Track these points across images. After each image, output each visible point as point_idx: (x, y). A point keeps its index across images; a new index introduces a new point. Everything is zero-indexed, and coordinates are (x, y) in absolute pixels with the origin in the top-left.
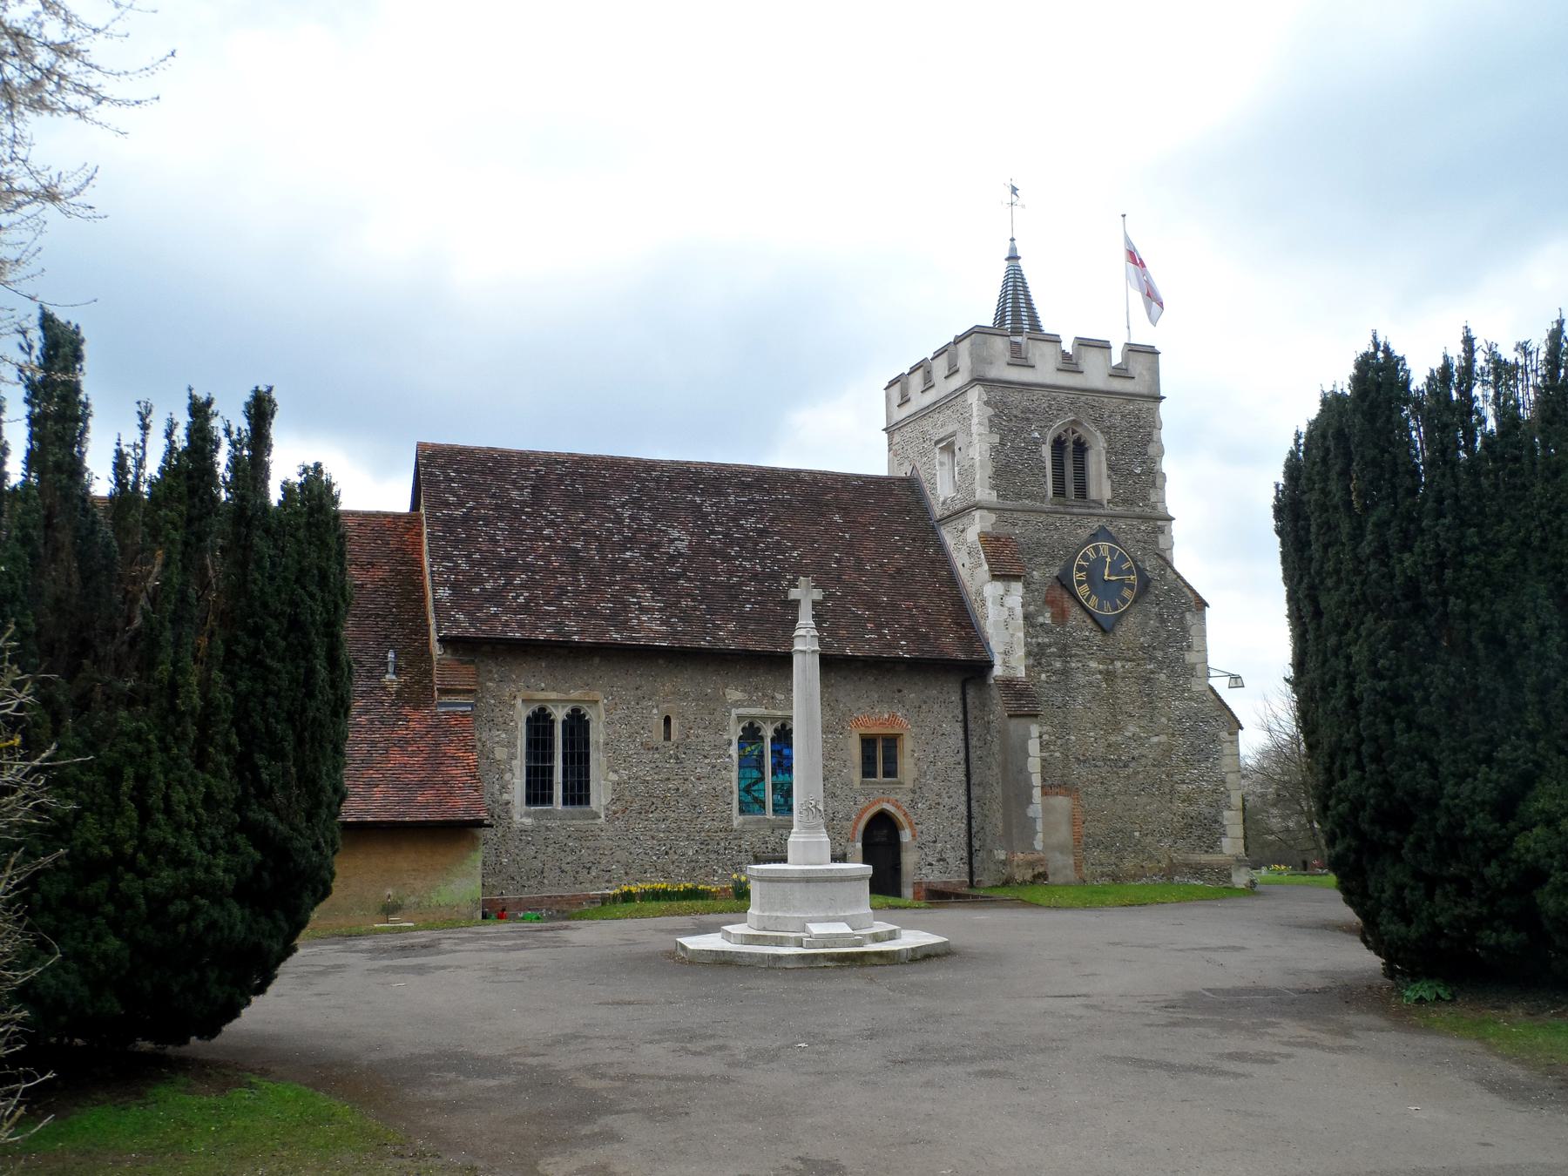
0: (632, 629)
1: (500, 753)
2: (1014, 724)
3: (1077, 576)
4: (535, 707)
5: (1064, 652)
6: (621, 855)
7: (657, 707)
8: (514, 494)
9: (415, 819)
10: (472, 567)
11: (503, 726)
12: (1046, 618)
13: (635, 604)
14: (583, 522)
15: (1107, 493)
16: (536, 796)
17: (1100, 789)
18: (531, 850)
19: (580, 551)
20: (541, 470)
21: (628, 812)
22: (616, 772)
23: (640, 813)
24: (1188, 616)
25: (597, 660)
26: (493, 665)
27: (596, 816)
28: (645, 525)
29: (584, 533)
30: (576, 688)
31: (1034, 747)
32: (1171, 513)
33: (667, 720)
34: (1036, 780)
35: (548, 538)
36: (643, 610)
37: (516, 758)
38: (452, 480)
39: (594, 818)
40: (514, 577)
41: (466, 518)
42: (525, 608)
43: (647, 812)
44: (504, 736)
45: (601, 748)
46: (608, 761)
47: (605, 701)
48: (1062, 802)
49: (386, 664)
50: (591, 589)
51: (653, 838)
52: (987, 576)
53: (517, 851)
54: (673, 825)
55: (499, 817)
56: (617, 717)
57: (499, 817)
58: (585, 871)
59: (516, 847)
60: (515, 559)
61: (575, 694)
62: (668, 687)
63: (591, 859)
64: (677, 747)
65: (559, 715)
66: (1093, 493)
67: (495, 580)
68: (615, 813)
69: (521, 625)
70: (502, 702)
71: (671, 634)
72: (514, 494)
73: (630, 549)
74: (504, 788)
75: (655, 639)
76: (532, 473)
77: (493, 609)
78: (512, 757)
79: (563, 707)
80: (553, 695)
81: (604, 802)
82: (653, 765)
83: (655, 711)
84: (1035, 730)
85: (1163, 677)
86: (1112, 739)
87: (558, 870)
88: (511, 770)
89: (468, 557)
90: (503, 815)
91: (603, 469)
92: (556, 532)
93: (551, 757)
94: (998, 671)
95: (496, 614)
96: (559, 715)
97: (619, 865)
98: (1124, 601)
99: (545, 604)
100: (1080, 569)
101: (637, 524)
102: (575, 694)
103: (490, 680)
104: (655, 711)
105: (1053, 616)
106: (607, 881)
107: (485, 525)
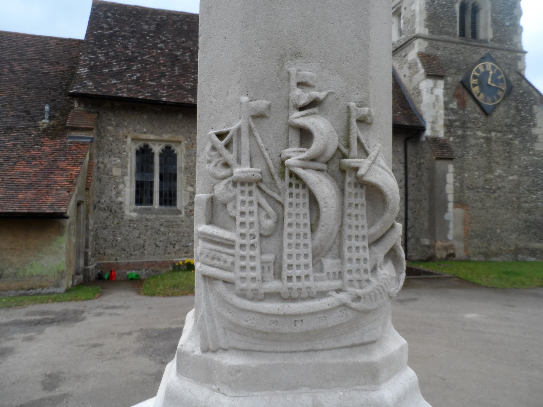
1: (116, 172)
2: (439, 163)
3: (473, 81)
4: (141, 144)
5: (464, 125)
8: (145, 27)
12: (454, 105)
14: (183, 42)
15: (490, 36)
17: (480, 205)
18: (136, 233)
19: (179, 56)
20: (164, 18)
24: (535, 107)
25: (180, 116)
27: (179, 212)
29: (184, 48)
30: (167, 133)
31: (450, 178)
32: (525, 48)
34: (451, 198)
35: (161, 49)
38: (109, 17)
39: (177, 214)
40: (133, 66)
41: (111, 36)
42: (136, 82)
44: (119, 161)
45: (183, 171)
46: (187, 179)
47: (186, 142)
48: (460, 211)
49: (44, 114)
50: (181, 75)
52: (423, 77)
53: (127, 233)
58: (172, 246)
59: (127, 231)
61: (166, 137)
63: (176, 239)
65: (157, 149)
66: (482, 35)
67: (120, 66)
69: (130, 90)
72: (145, 27)
74: (118, 194)
76: (159, 18)
77: (114, 81)
78: (124, 174)
79: (160, 145)
80: (152, 137)
81: (184, 204)
84: (451, 168)
85: (517, 142)
86: (488, 176)
87: (154, 246)
88: (123, 183)
89: (106, 54)
90: (118, 210)
92: (166, 46)
93: (152, 176)
94: (428, 133)
95: (115, 84)
96: (157, 149)
98: (498, 97)
100: (475, 77)
102: (166, 137)
103: (110, 125)
105: (458, 104)
107: (122, 40)
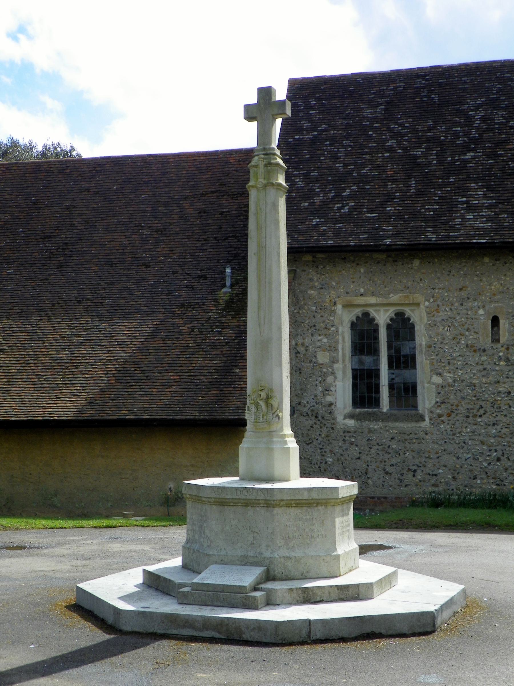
0: (453, 228)
1: (322, 358)
4: (358, 312)
6: (450, 460)
7: (484, 307)
8: (368, 113)
9: (184, 417)
10: (307, 184)
11: (324, 332)
13: (463, 203)
14: (429, 129)
16: (362, 398)
18: (354, 451)
19: (419, 158)
20: (400, 87)
21: (453, 415)
22: (439, 374)
23: (468, 417)
25: (416, 263)
26: (313, 273)
27: (422, 418)
28: (496, 124)
30: (395, 291)
33: (495, 321)
35: (390, 150)
36: (470, 208)
37: (337, 361)
38: (312, 108)
39: (417, 421)
40: (344, 189)
41: (314, 141)
42: (347, 218)
43: (475, 416)
44: (325, 340)
45: (424, 350)
46: (432, 364)
47: (427, 303)
49: (223, 279)
50: (419, 193)
51: (482, 443)
53: (341, 451)
54: (504, 430)
55: (323, 418)
56: (439, 319)
57: (323, 418)
58: (411, 474)
59: (340, 447)
60: (350, 173)
61: (394, 298)
62: (496, 286)
63: (417, 461)
64: (508, 349)
67: (325, 194)
68: (440, 416)
69: (337, 233)
70: (323, 308)
71: (496, 230)
72: (368, 113)
73: (474, 150)
74: (327, 390)
75: (474, 236)
76: (391, 90)
77: (315, 221)
78: (334, 361)
79: (386, 311)
80: (373, 300)
81: (428, 405)
82: (481, 367)
83: (481, 312)
87: (382, 472)
88: (333, 373)
89: (306, 176)
90: (327, 416)
91: (465, 76)
92: (399, 143)
93: (377, 362)
97: (446, 469)
99: (368, 212)
101: (488, 124)
102: (394, 298)
103: (312, 288)
104: (481, 312)
106: (433, 485)
107: (330, 145)
